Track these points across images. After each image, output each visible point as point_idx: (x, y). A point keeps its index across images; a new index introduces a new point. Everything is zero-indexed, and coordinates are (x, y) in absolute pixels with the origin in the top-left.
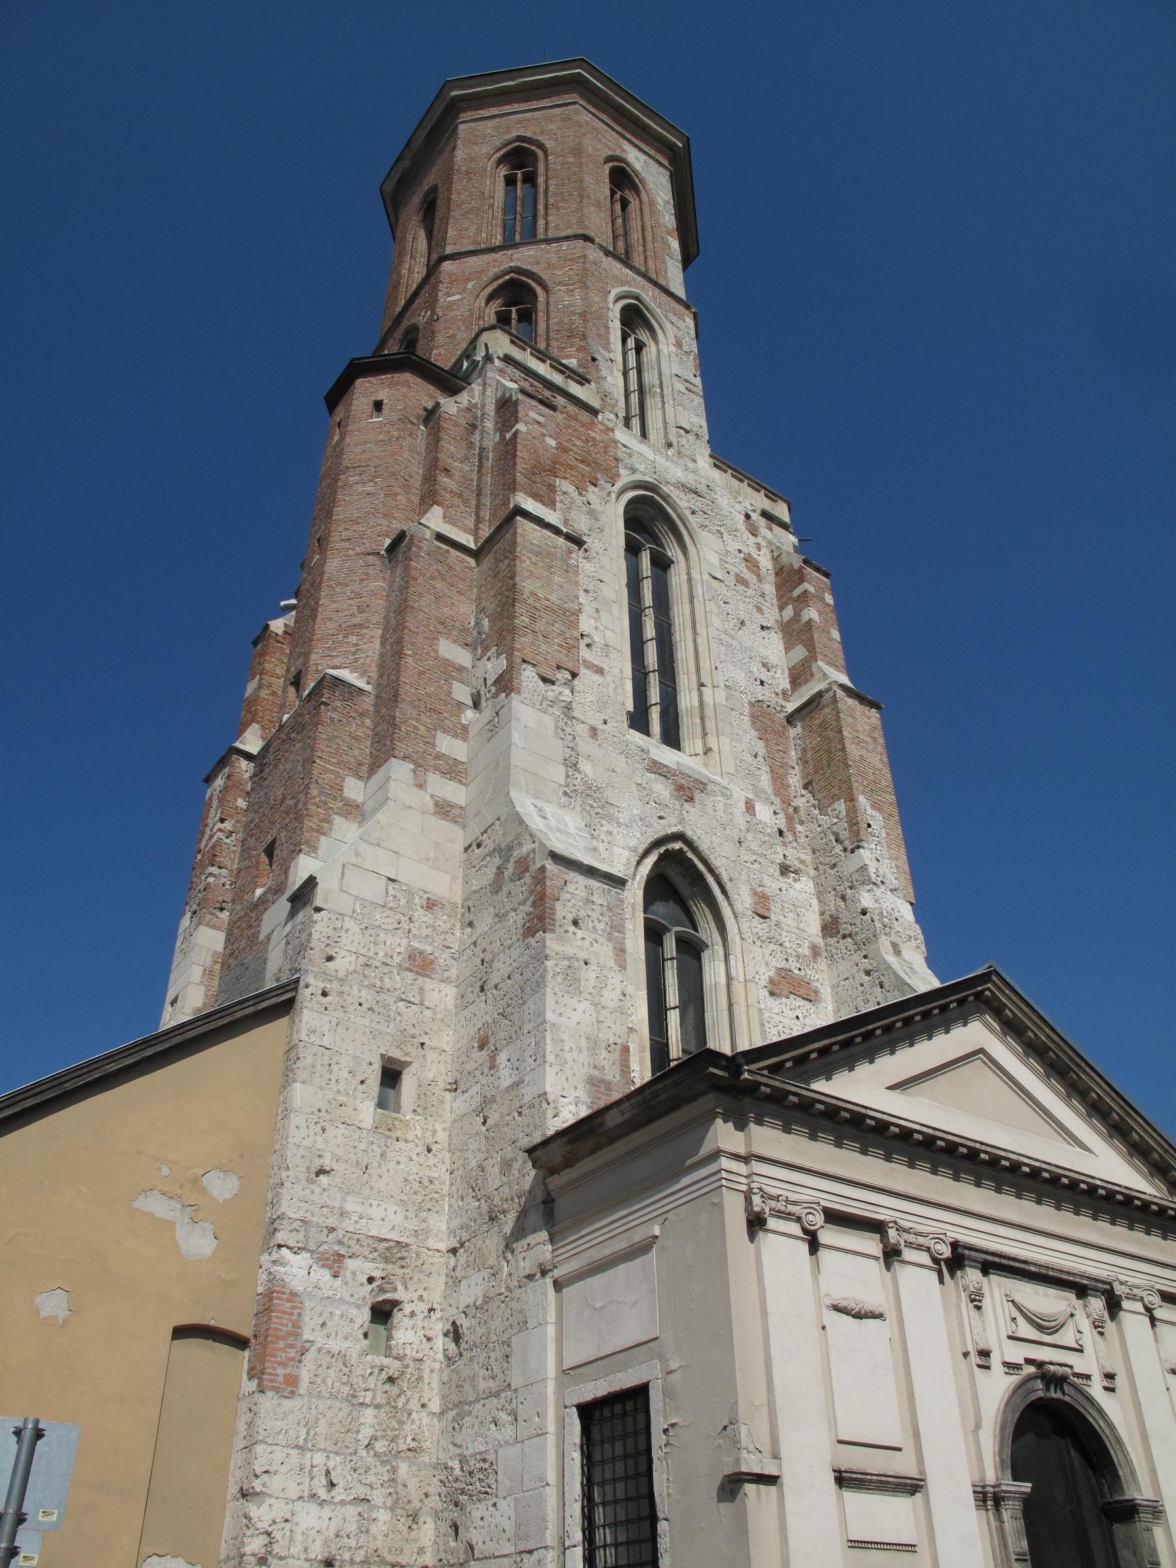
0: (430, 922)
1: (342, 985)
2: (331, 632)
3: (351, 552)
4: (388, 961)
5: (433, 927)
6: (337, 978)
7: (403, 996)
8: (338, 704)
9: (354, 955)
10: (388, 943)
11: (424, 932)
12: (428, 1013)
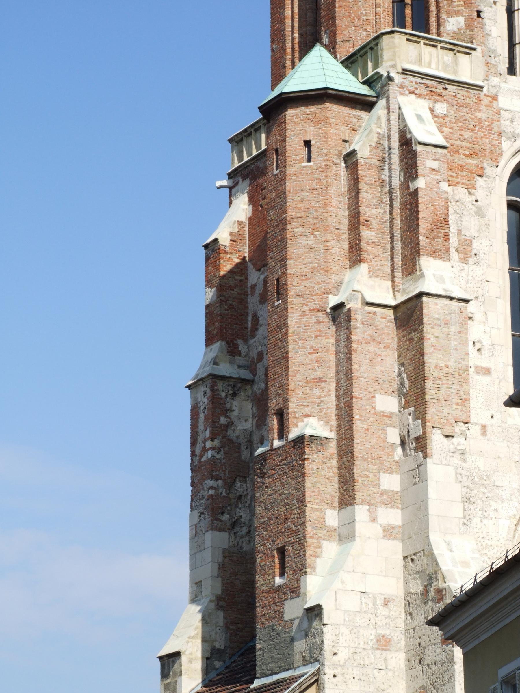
0: (387, 614)
1: (343, 669)
2: (301, 384)
3: (305, 308)
4: (366, 647)
5: (389, 617)
6: (340, 665)
7: (376, 667)
8: (315, 456)
9: (347, 649)
10: (365, 635)
11: (385, 621)
12: (390, 674)
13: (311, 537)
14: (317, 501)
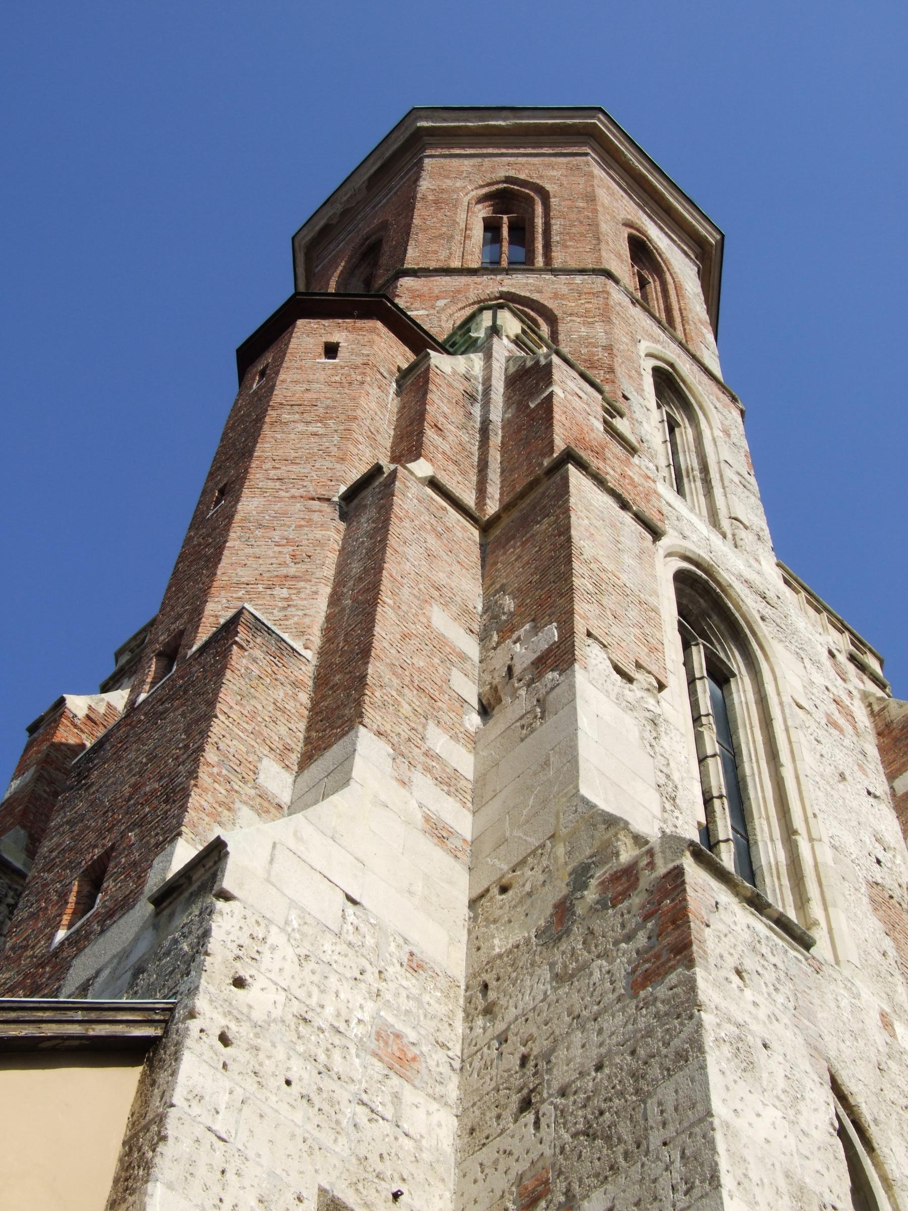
0: (415, 991)
1: (257, 1035)
4: (342, 1027)
5: (418, 1000)
6: (249, 1018)
7: (365, 1097)
9: (284, 994)
10: (342, 996)
11: (405, 1004)
12: (407, 1144)
13: (211, 775)
14: (245, 725)
